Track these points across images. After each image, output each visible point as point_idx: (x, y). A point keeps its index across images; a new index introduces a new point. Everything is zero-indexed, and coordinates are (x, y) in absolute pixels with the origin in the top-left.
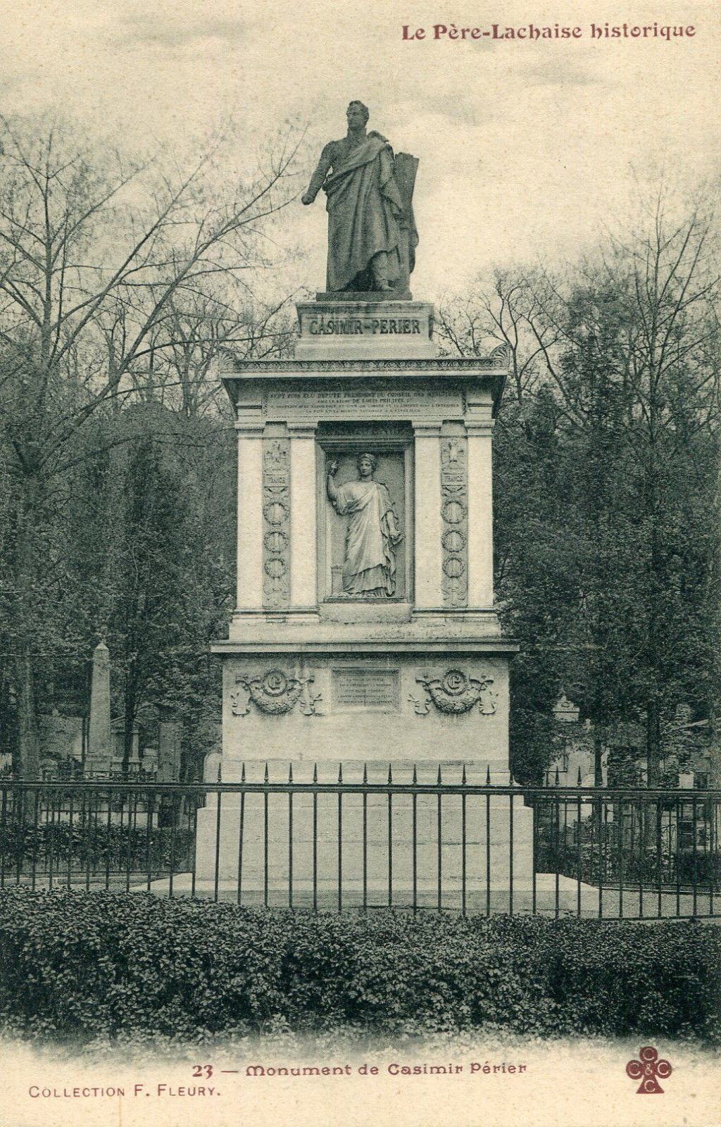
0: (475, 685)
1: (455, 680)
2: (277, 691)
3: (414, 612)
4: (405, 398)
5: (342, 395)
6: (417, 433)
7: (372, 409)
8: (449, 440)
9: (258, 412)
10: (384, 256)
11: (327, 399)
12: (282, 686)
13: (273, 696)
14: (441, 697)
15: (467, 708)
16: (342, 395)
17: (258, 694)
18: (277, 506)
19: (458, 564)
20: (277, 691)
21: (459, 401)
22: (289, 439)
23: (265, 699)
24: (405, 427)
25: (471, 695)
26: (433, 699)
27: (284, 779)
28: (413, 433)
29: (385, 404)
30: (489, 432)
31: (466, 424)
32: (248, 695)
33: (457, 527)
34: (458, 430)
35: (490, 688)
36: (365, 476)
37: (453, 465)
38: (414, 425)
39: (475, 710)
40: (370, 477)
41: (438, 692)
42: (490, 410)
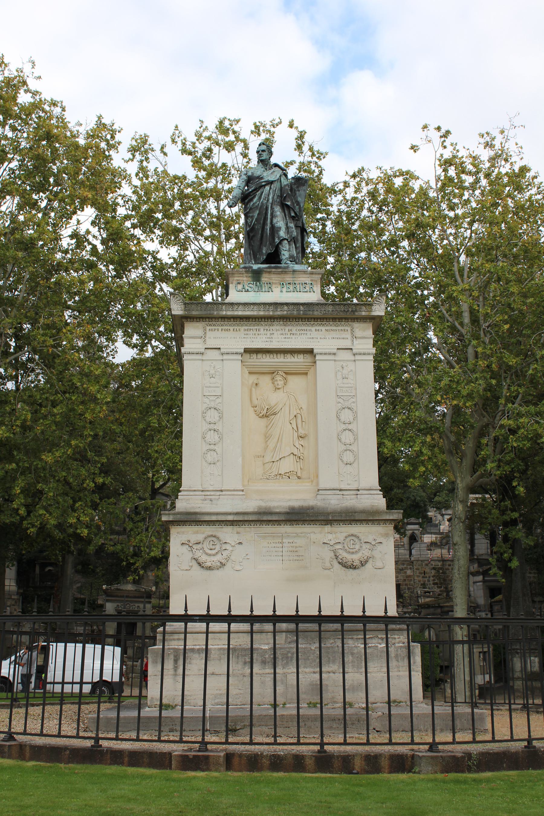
0: (368, 546)
1: (352, 542)
2: (213, 552)
3: (319, 490)
4: (308, 333)
5: (262, 330)
6: (318, 357)
7: (284, 340)
8: (342, 363)
9: (199, 341)
10: (286, 242)
11: (251, 332)
12: (218, 547)
13: (210, 555)
14: (343, 555)
15: (363, 564)
16: (262, 330)
17: (198, 554)
18: (212, 410)
19: (351, 454)
20: (213, 552)
21: (349, 335)
22: (222, 360)
23: (203, 558)
24: (310, 352)
25: (365, 552)
26: (337, 557)
27: (214, 626)
28: (315, 356)
29: (293, 337)
30: (371, 358)
31: (354, 351)
32: (190, 555)
33: (350, 427)
34: (347, 355)
35: (379, 548)
36: (279, 389)
37: (345, 380)
38: (315, 351)
39: (369, 566)
40: (282, 390)
41: (341, 552)
42: (371, 341)
